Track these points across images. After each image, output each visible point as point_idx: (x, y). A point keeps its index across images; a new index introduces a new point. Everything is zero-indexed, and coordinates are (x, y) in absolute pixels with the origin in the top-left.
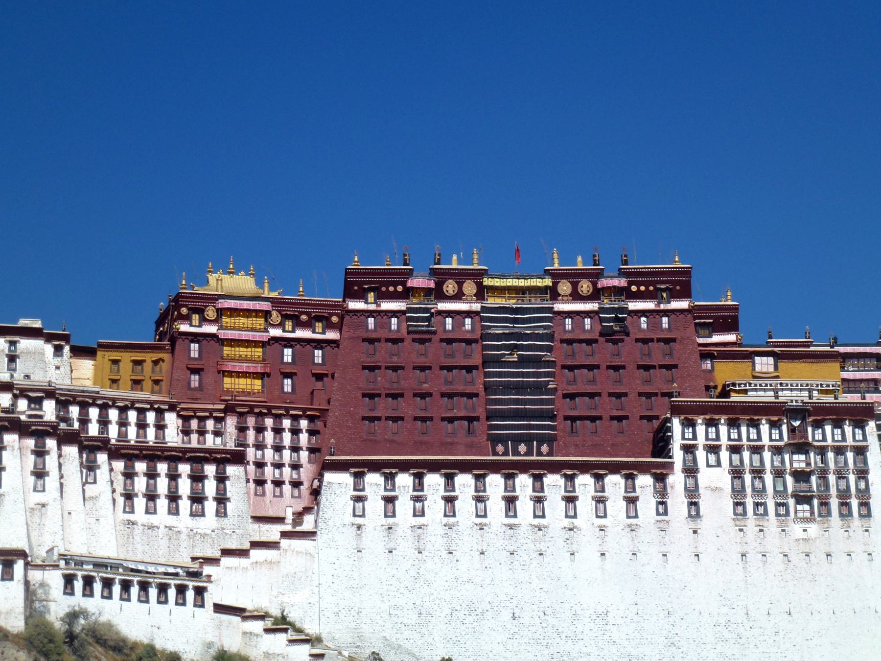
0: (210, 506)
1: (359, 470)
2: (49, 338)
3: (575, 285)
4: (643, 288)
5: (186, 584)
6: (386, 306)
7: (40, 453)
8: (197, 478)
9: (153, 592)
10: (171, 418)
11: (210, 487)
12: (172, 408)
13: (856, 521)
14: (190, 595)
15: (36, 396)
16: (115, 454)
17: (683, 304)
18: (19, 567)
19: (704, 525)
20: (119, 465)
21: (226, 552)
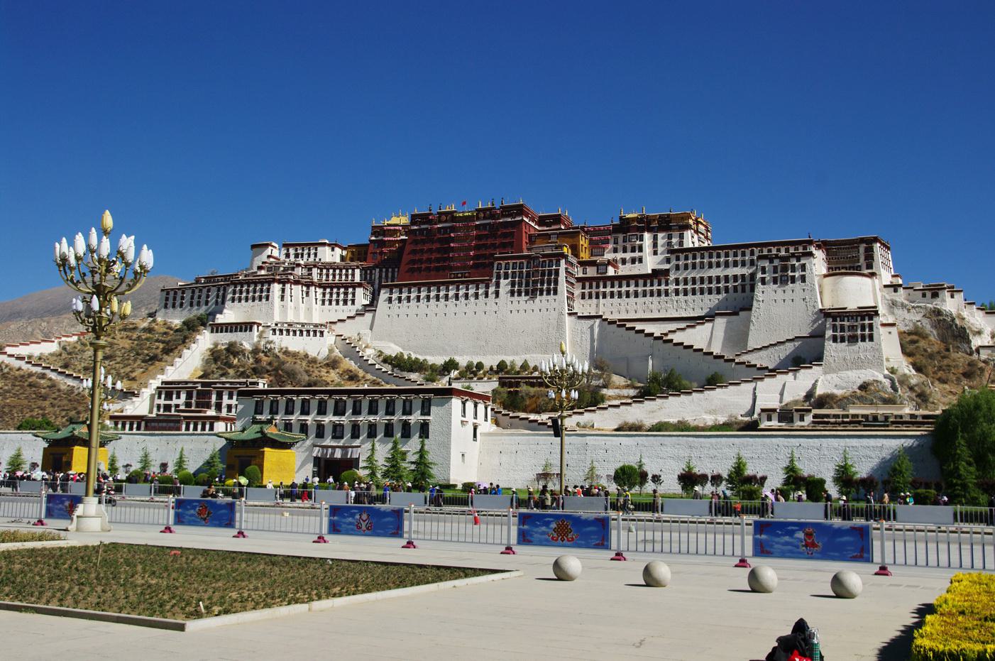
0: (349, 303)
1: (391, 288)
2: (329, 245)
3: (484, 214)
5: (317, 330)
6: (423, 227)
7: (283, 290)
8: (346, 294)
9: (305, 333)
10: (357, 272)
11: (350, 297)
12: (358, 267)
13: (552, 297)
14: (318, 334)
15: (309, 267)
16: (320, 286)
17: (521, 218)
18: (255, 327)
19: (497, 300)
20: (321, 290)
21: (349, 317)
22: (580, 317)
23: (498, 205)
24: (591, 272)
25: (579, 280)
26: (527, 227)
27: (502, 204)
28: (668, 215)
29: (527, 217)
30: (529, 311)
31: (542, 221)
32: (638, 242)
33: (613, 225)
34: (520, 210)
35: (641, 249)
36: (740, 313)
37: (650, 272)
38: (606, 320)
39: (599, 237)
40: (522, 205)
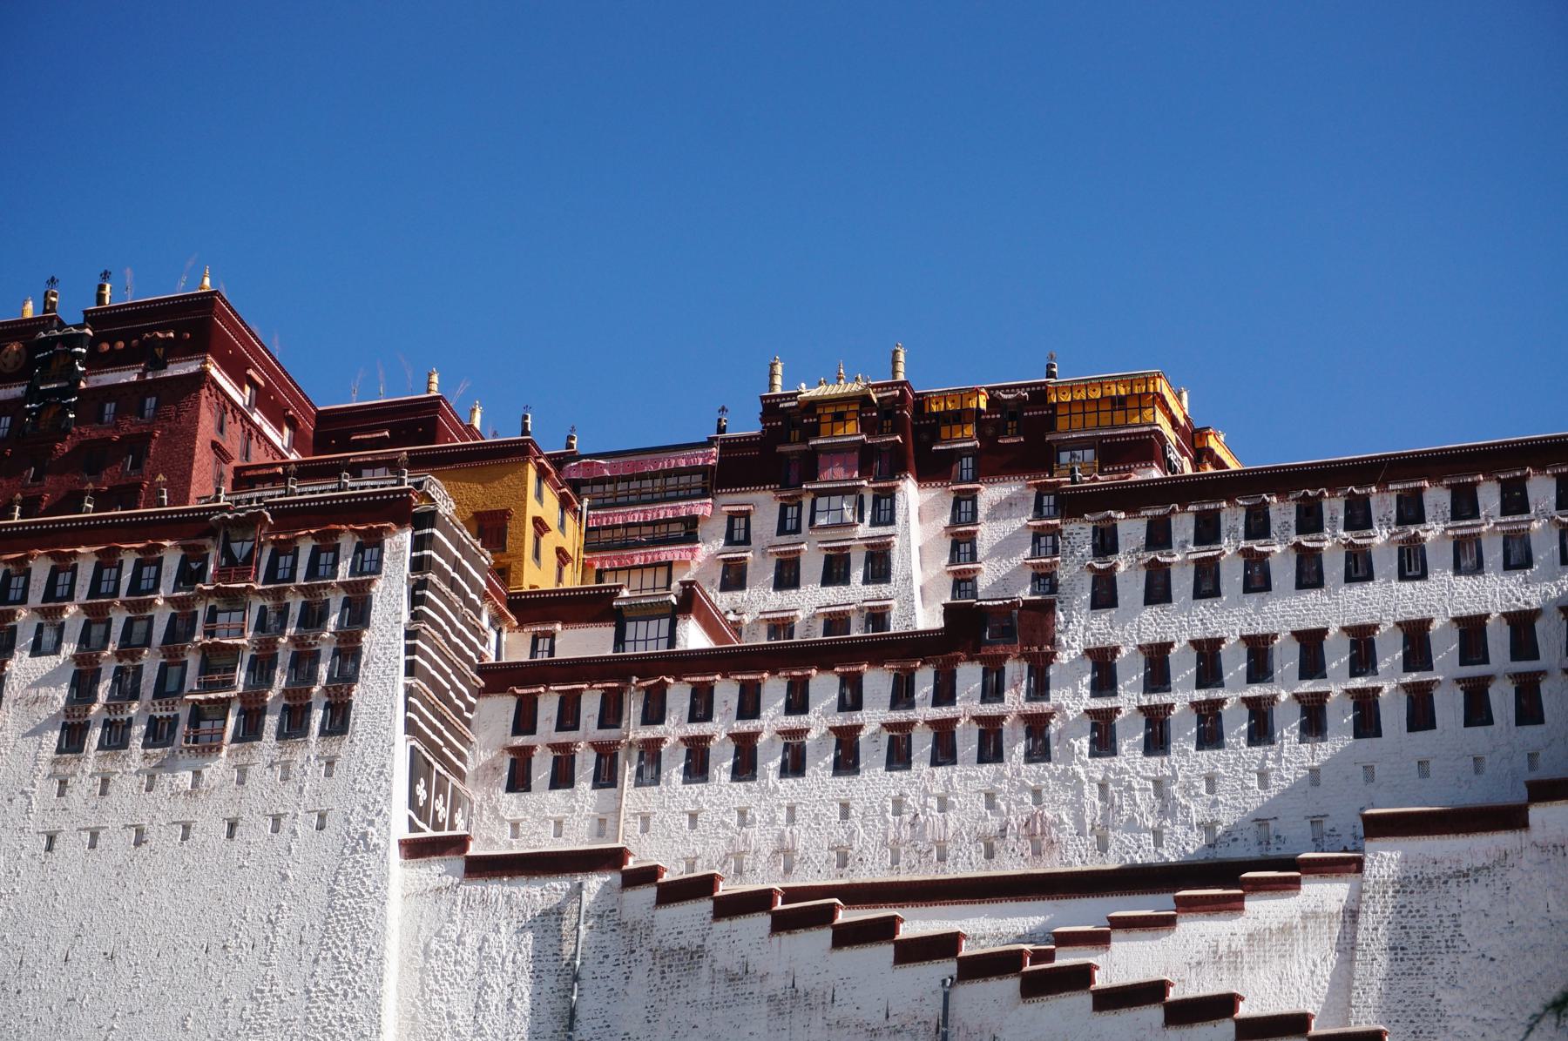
4: (121, 345)
17: (193, 367)
22: (484, 868)
23: (71, 312)
24: (581, 642)
25: (497, 678)
26: (234, 429)
27: (100, 298)
28: (1039, 394)
29: (241, 380)
30: (163, 838)
31: (334, 433)
32: (864, 530)
33: (728, 446)
34: (196, 323)
35: (879, 565)
36: (1536, 813)
37: (939, 623)
38: (648, 875)
39: (627, 491)
40: (206, 303)
